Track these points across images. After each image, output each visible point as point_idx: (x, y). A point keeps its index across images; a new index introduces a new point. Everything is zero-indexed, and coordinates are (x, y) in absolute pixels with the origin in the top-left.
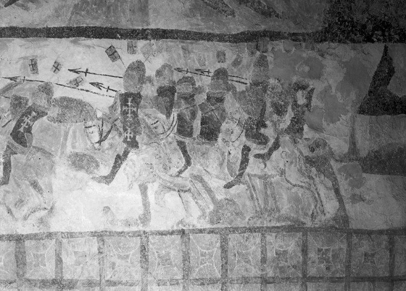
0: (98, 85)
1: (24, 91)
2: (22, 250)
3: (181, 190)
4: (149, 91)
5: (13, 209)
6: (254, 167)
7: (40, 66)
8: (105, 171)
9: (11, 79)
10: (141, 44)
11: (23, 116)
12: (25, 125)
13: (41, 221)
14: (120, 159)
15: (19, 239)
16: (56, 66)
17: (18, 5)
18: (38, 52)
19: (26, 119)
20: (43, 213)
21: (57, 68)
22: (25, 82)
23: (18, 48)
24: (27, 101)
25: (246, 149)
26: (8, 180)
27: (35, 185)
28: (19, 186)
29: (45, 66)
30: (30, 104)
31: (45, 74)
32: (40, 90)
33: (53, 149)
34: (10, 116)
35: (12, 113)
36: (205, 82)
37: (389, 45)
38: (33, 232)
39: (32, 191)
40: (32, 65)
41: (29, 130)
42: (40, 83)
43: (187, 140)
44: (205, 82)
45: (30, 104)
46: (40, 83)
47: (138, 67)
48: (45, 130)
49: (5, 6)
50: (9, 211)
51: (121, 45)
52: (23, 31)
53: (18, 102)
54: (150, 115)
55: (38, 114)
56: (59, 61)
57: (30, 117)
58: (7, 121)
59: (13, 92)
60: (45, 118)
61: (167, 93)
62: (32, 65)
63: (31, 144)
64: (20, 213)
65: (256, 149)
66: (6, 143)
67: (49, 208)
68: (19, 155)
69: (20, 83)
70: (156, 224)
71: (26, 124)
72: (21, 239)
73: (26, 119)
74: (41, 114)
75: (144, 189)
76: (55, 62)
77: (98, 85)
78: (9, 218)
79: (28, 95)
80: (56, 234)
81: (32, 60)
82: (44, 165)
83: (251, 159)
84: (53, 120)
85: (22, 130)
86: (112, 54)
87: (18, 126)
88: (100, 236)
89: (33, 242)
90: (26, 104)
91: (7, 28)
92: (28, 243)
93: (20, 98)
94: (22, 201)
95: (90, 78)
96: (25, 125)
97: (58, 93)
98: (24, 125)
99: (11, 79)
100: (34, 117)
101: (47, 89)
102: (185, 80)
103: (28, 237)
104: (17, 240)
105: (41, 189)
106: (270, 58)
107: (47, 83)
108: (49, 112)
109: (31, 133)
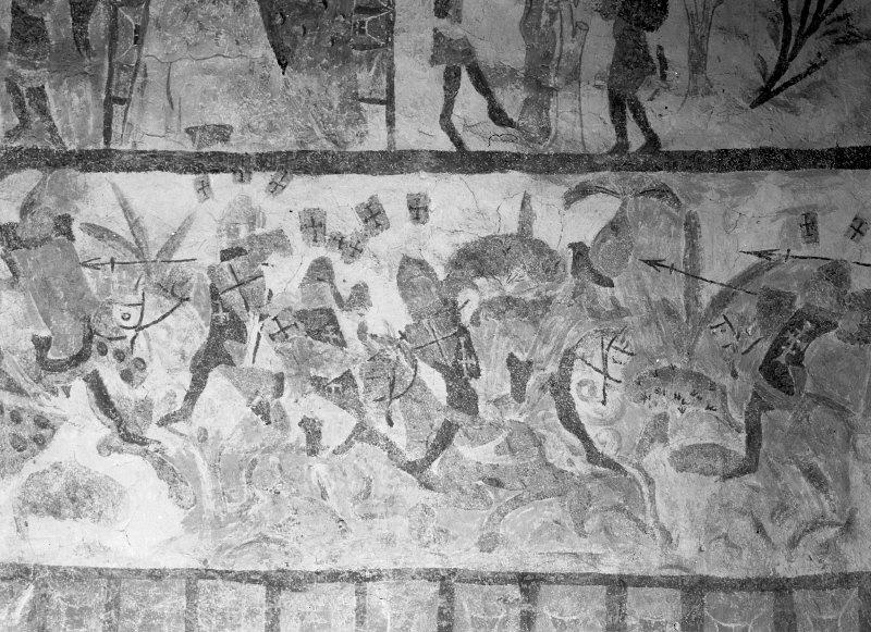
1: (792, 279)
2: (788, 611)
5: (768, 526)
7: (822, 229)
9: (759, 255)
11: (784, 330)
12: (789, 351)
13: (826, 547)
15: (779, 588)
16: (856, 226)
17: (777, 104)
18: (819, 199)
19: (791, 337)
20: (831, 532)
21: (858, 230)
22: (790, 260)
23: (777, 192)
24: (793, 299)
26: (757, 463)
27: (813, 475)
28: (777, 475)
30: (799, 304)
32: (821, 277)
33: (848, 398)
34: (759, 331)
35: (763, 326)
38: (811, 573)
39: (805, 486)
40: (807, 224)
41: (797, 359)
42: (823, 263)
45: (799, 304)
46: (823, 263)
48: (828, 359)
49: (752, 107)
50: (759, 529)
52: (787, 156)
53: (774, 302)
55: (818, 326)
56: (865, 215)
57: (801, 333)
58: (752, 341)
59: (765, 281)
60: (833, 333)
62: (807, 224)
63: (802, 388)
66: (751, 387)
67: (843, 522)
68: (777, 411)
69: (778, 263)
71: (791, 347)
72: (784, 587)
73: (791, 337)
74: (823, 326)
76: (856, 219)
78: (761, 543)
79: (794, 287)
80: (859, 575)
81: (806, 216)
82: (830, 431)
84: (850, 338)
85: (782, 359)
87: (775, 351)
89: (810, 595)
90: (791, 306)
91: (754, 150)
92: (797, 596)
93: (779, 294)
94: (786, 508)
96: (789, 351)
98: (787, 350)
99: (759, 255)
100: (809, 333)
103: (800, 583)
104: (776, 590)
105: (826, 482)
107: (837, 261)
108: (840, 323)
109: (802, 366)
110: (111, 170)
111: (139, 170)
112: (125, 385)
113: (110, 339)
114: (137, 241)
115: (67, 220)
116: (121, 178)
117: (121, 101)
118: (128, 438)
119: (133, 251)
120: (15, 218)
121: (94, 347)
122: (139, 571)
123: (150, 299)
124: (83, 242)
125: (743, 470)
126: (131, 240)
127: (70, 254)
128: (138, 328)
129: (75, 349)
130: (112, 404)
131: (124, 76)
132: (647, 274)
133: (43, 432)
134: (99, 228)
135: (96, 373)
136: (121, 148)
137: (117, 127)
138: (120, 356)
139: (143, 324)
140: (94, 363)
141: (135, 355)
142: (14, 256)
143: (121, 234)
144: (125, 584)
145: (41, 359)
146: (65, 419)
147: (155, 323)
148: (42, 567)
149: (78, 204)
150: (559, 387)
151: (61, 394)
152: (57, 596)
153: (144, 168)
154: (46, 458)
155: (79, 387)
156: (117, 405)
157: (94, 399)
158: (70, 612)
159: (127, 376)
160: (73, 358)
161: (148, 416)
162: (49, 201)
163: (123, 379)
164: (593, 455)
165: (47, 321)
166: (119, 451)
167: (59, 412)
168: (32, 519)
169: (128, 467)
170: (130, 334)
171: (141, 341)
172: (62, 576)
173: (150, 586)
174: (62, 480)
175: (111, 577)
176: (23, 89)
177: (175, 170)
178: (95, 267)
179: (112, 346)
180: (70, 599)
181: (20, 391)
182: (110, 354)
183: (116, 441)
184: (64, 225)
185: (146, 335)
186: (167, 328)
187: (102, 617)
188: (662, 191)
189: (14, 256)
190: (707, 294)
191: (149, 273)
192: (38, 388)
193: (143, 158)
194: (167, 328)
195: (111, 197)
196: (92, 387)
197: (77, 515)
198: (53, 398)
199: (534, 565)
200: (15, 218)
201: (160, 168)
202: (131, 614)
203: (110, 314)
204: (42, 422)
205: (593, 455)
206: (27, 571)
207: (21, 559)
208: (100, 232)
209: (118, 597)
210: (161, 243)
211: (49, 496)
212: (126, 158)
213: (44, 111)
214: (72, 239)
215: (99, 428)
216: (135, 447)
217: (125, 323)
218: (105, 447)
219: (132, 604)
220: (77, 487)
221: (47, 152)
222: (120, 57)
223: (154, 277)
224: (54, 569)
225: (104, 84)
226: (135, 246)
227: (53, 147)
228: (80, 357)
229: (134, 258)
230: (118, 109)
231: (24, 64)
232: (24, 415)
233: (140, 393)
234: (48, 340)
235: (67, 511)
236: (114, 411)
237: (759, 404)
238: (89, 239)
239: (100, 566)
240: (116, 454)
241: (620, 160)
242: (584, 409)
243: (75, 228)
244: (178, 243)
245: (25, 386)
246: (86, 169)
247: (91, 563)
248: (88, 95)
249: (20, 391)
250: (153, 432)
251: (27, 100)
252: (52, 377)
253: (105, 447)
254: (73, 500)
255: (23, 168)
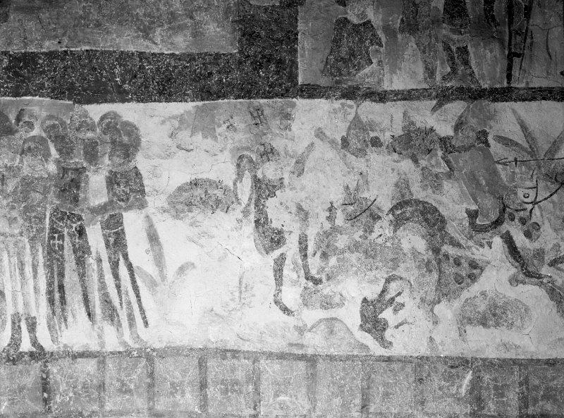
110: (512, 101)
111: (530, 100)
112: (527, 241)
113: (517, 211)
114: (530, 147)
115: (485, 133)
116: (519, 106)
117: (518, 55)
118: (529, 275)
119: (529, 153)
120: (451, 133)
121: (506, 216)
122: (539, 360)
123: (541, 184)
124: (496, 148)
126: (526, 145)
127: (487, 156)
128: (534, 203)
129: (494, 217)
130: (519, 253)
131: (519, 38)
133: (475, 271)
134: (505, 139)
135: (508, 232)
136: (518, 86)
137: (516, 72)
138: (523, 221)
139: (538, 200)
140: (506, 227)
141: (533, 221)
142: (450, 157)
143: (520, 142)
144: (530, 369)
145: (472, 224)
146: (488, 263)
147: (546, 199)
148: (476, 359)
149: (492, 123)
151: (486, 246)
152: (487, 377)
153: (533, 99)
154: (476, 288)
155: (498, 241)
156: (522, 253)
157: (507, 250)
158: (496, 388)
159: (528, 234)
160: (493, 223)
161: (542, 260)
162: (473, 122)
163: (525, 235)
165: (476, 201)
166: (524, 283)
167: (484, 258)
168: (468, 328)
169: (530, 293)
170: (529, 207)
171: (537, 211)
172: (489, 364)
173: (547, 370)
174: (487, 302)
175: (520, 365)
176: (454, 48)
177: (555, 99)
178: (504, 164)
179: (517, 215)
180: (495, 380)
181: (459, 245)
182: (516, 220)
183: (521, 277)
184: (482, 136)
185: (540, 207)
186: (553, 202)
187: (517, 390)
189: (450, 157)
191: (539, 167)
192: (470, 243)
193: (533, 92)
194: (553, 202)
195: (510, 114)
196: (506, 242)
197: (497, 325)
198: (481, 249)
200: (451, 133)
201: (544, 99)
202: (536, 388)
203: (516, 194)
204: (473, 265)
206: (467, 362)
207: (462, 354)
208: (505, 141)
209: (527, 377)
210: (546, 147)
211: (479, 312)
212: (521, 92)
213: (466, 63)
214: (488, 145)
215: (510, 269)
216: (533, 280)
217: (526, 200)
218: (514, 281)
219: (537, 382)
220: (496, 307)
221: (469, 90)
222: (515, 26)
223: (543, 169)
224: (484, 360)
225: (507, 44)
226: (530, 150)
227: (473, 86)
228: (497, 223)
229: (529, 158)
230: (516, 60)
231: (454, 31)
232: (463, 261)
233: (536, 245)
234: (476, 212)
235: (491, 323)
236: (520, 257)
238: (499, 145)
239: (514, 357)
240: (521, 285)
243: (490, 139)
244: (558, 147)
245: (462, 242)
246: (495, 100)
247: (508, 356)
248: (497, 52)
249: (459, 245)
250: (545, 270)
251: (456, 55)
252: (480, 236)
253: (514, 281)
254: (494, 315)
255: (454, 100)
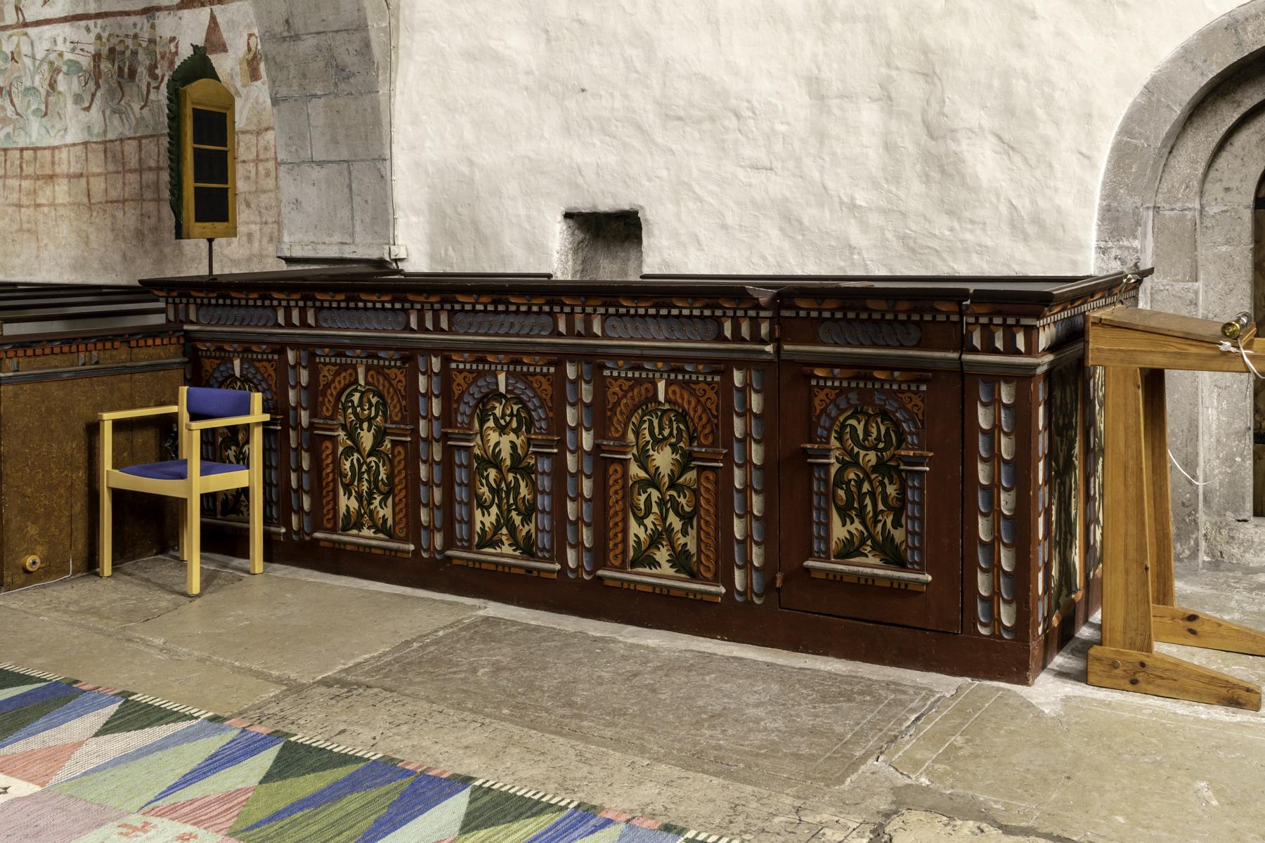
0: (82, 50)
1: (52, 57)
3: (120, 113)
4: (105, 51)
6: (153, 96)
8: (87, 104)
10: (99, 22)
14: (93, 95)
25: (149, 84)
29: (60, 40)
31: (61, 47)
36: (129, 42)
37: (213, 7)
43: (122, 80)
44: (129, 42)
47: (99, 37)
51: (91, 23)
53: (51, 63)
54: (105, 65)
61: (112, 50)
64: (52, 132)
65: (154, 84)
70: (110, 136)
75: (103, 112)
77: (82, 50)
83: (152, 90)
86: (88, 30)
88: (85, 144)
95: (80, 46)
97: (67, 56)
101: (61, 55)
102: (122, 41)
106: (157, 22)
125: (46, 114)
132: (24, 58)
150: (10, 93)
164: (18, 114)
188: (26, 34)
190: (37, 63)
199: (6, 146)
205: (18, 114)
237: (48, 94)
241: (17, 26)
242: (15, 100)
